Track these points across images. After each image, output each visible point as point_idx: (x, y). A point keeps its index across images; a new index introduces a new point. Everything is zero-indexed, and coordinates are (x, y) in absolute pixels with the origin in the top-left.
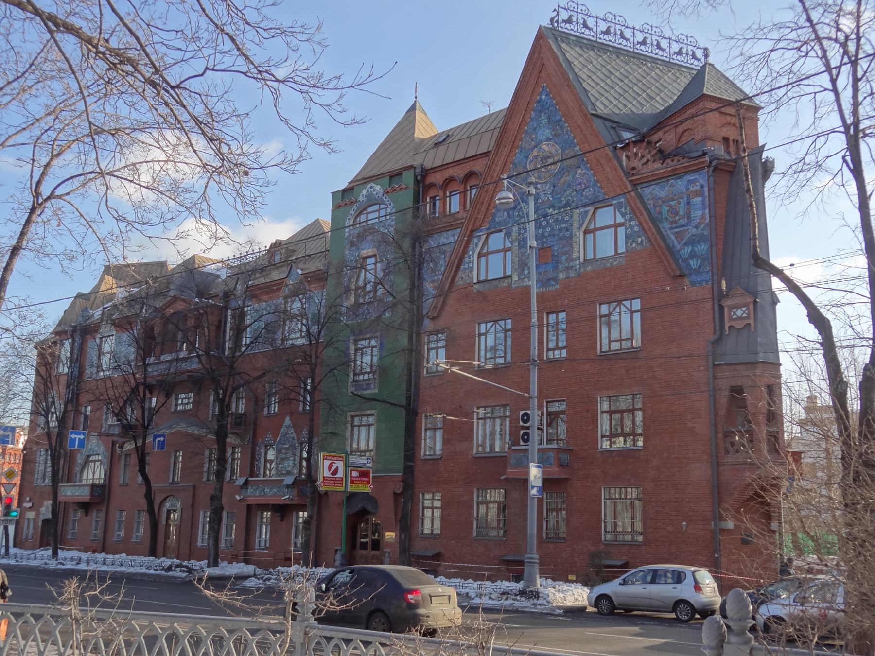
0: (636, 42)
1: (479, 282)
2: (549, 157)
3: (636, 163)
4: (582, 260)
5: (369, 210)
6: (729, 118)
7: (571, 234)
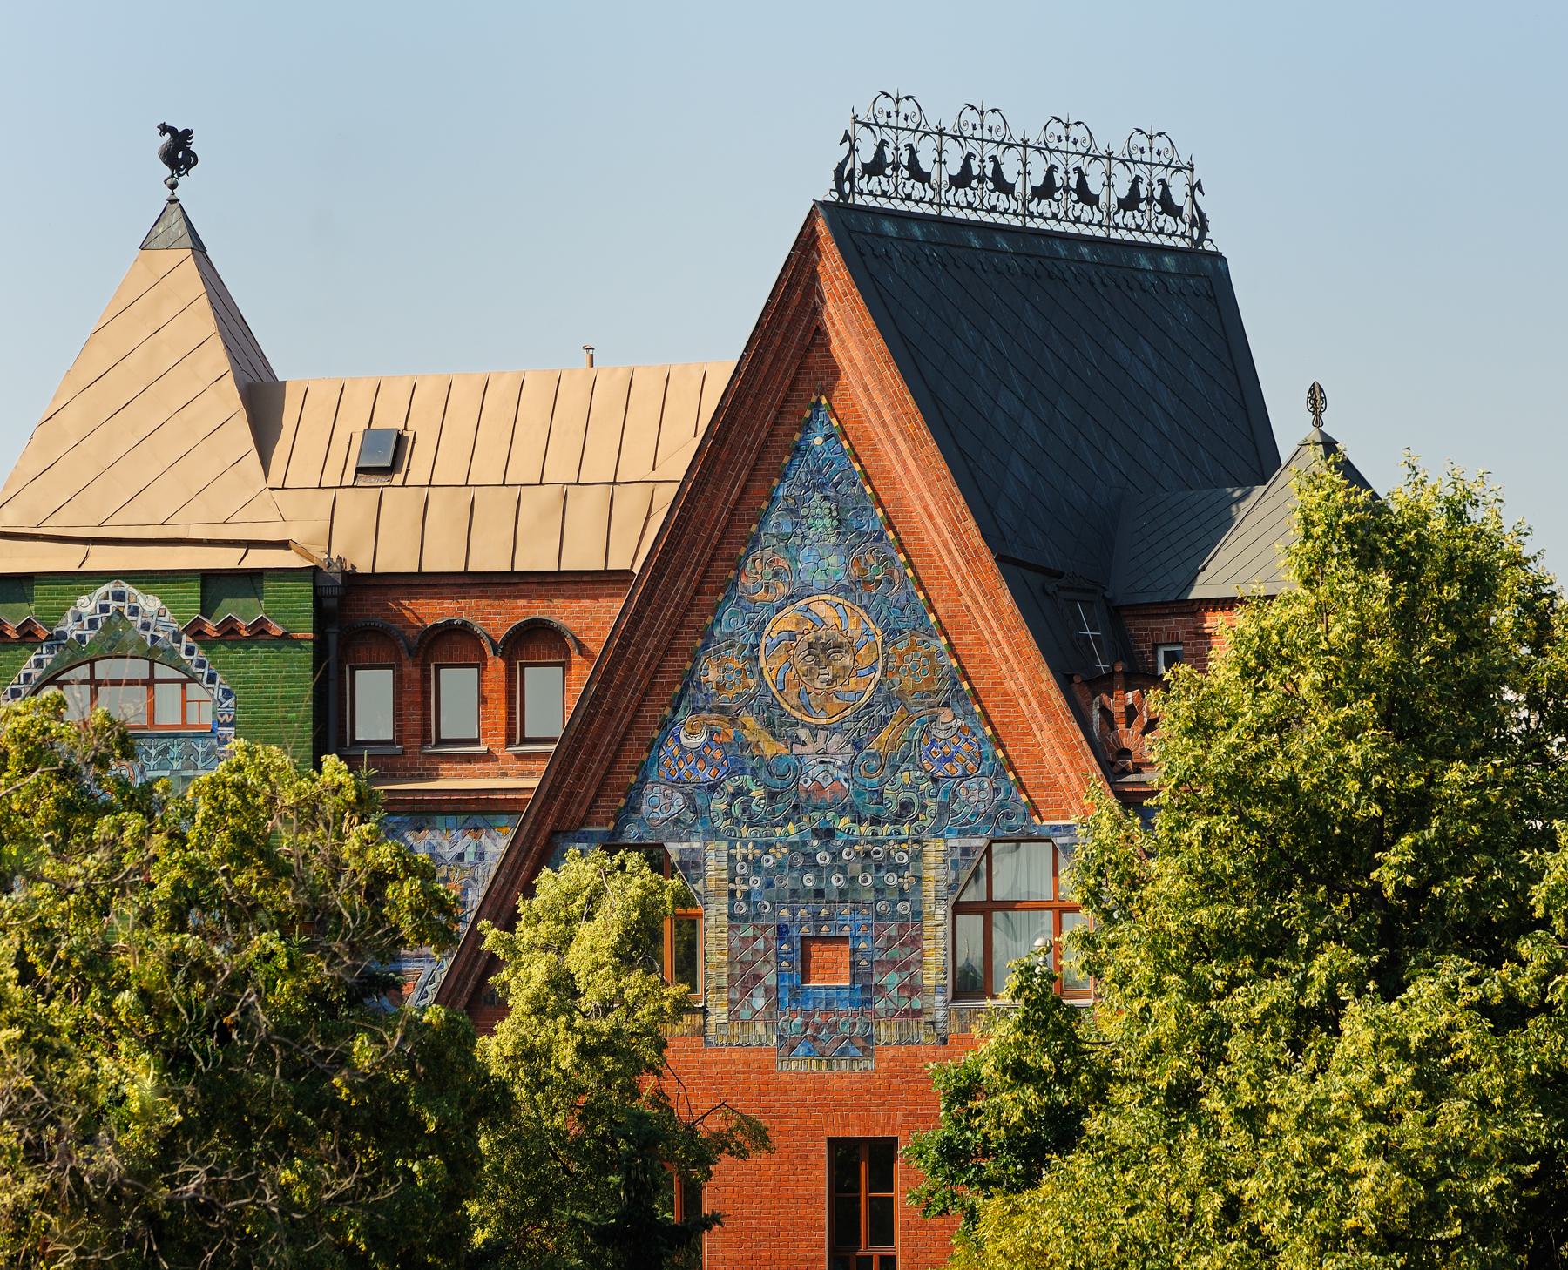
2: (838, 647)
5: (103, 670)
7: (917, 914)
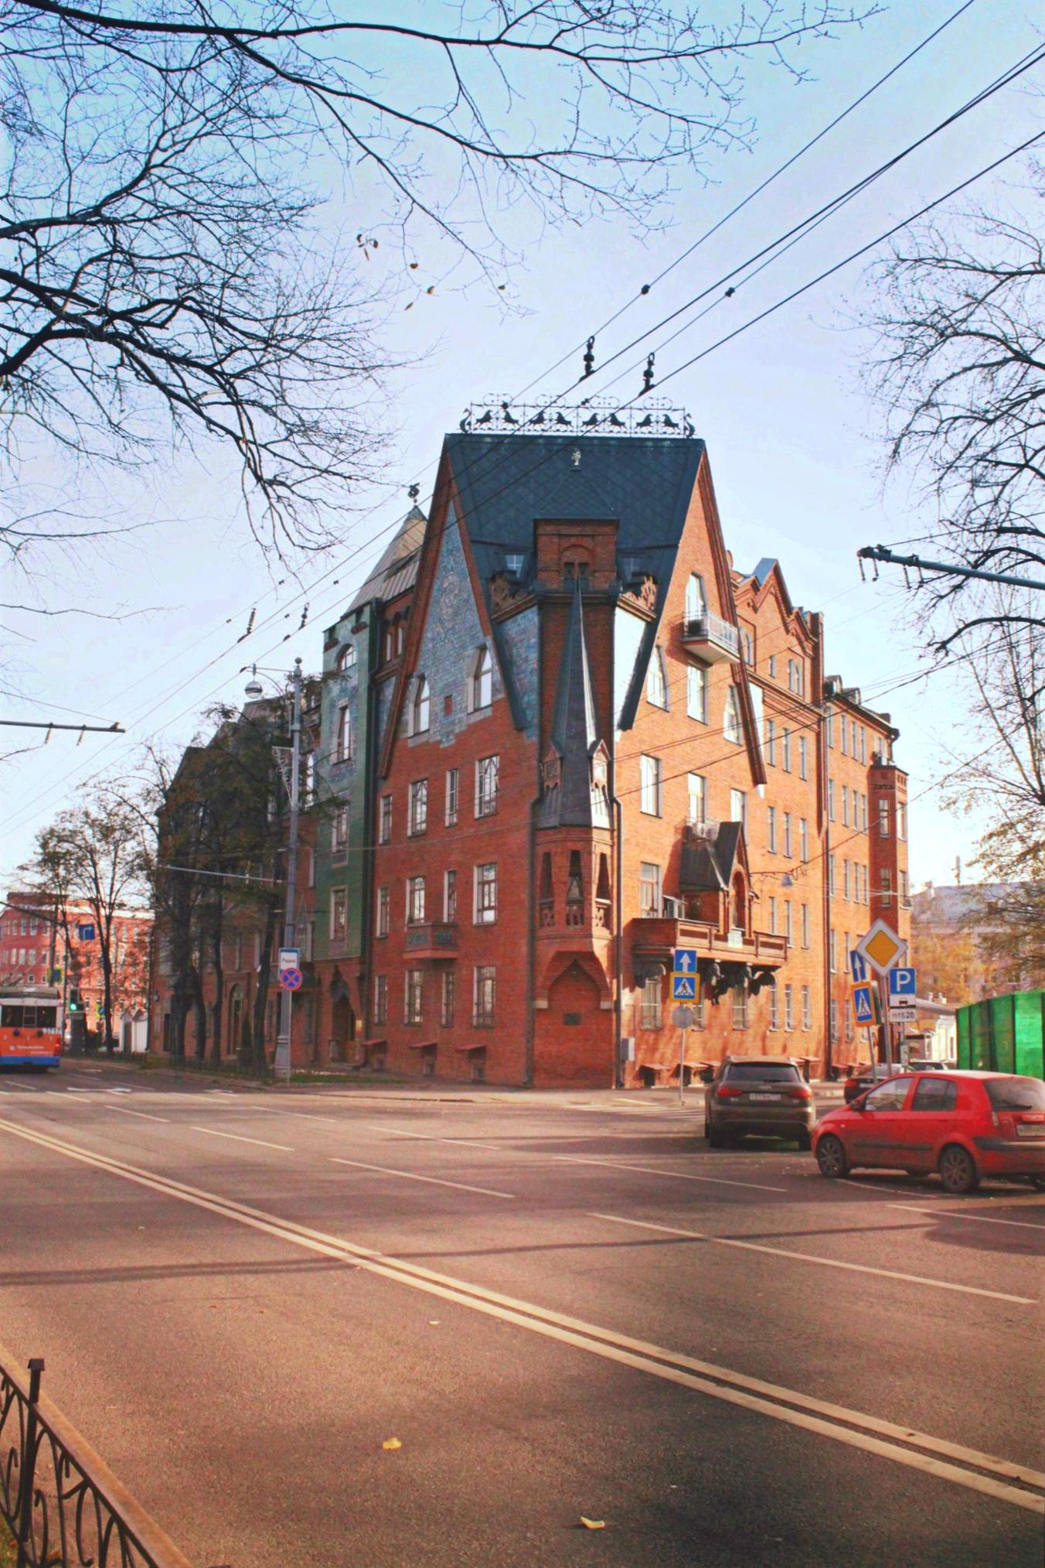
0: (581, 424)
1: (417, 734)
3: (498, 600)
4: (471, 709)
6: (573, 540)
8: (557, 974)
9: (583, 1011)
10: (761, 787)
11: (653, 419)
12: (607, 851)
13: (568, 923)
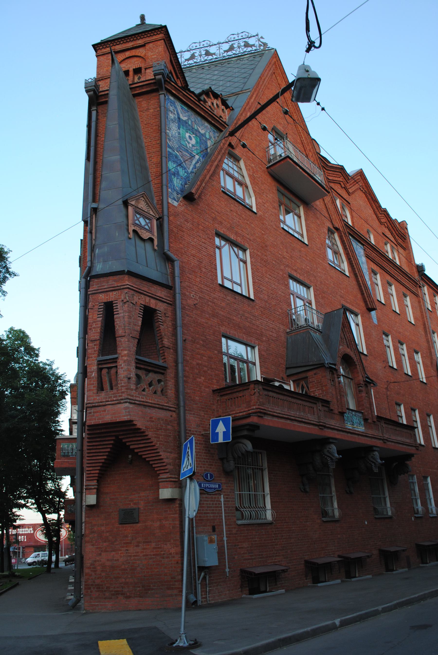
6: (128, 54)
8: (102, 458)
9: (142, 505)
10: (373, 313)
11: (235, 46)
12: (161, 307)
13: (101, 388)
